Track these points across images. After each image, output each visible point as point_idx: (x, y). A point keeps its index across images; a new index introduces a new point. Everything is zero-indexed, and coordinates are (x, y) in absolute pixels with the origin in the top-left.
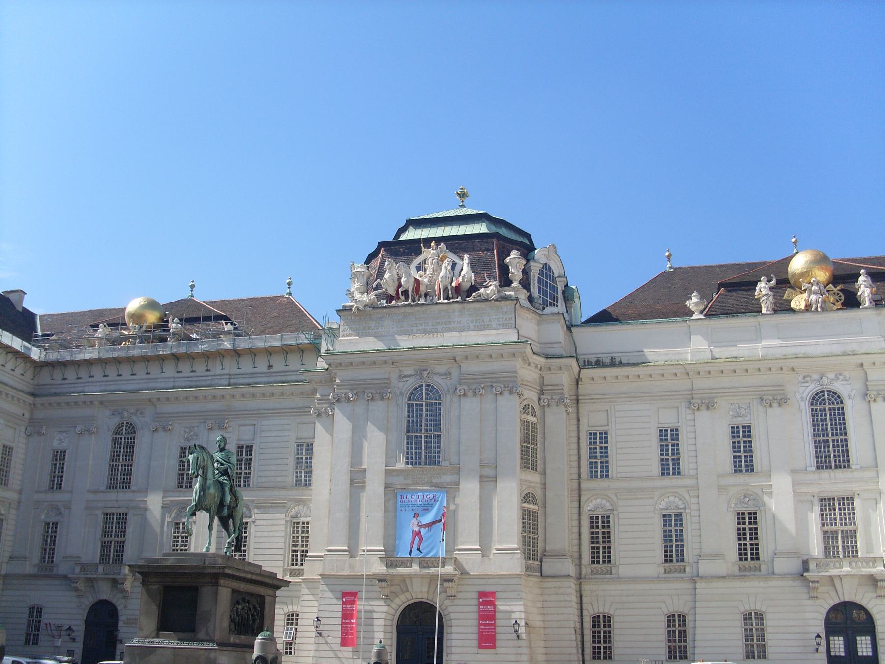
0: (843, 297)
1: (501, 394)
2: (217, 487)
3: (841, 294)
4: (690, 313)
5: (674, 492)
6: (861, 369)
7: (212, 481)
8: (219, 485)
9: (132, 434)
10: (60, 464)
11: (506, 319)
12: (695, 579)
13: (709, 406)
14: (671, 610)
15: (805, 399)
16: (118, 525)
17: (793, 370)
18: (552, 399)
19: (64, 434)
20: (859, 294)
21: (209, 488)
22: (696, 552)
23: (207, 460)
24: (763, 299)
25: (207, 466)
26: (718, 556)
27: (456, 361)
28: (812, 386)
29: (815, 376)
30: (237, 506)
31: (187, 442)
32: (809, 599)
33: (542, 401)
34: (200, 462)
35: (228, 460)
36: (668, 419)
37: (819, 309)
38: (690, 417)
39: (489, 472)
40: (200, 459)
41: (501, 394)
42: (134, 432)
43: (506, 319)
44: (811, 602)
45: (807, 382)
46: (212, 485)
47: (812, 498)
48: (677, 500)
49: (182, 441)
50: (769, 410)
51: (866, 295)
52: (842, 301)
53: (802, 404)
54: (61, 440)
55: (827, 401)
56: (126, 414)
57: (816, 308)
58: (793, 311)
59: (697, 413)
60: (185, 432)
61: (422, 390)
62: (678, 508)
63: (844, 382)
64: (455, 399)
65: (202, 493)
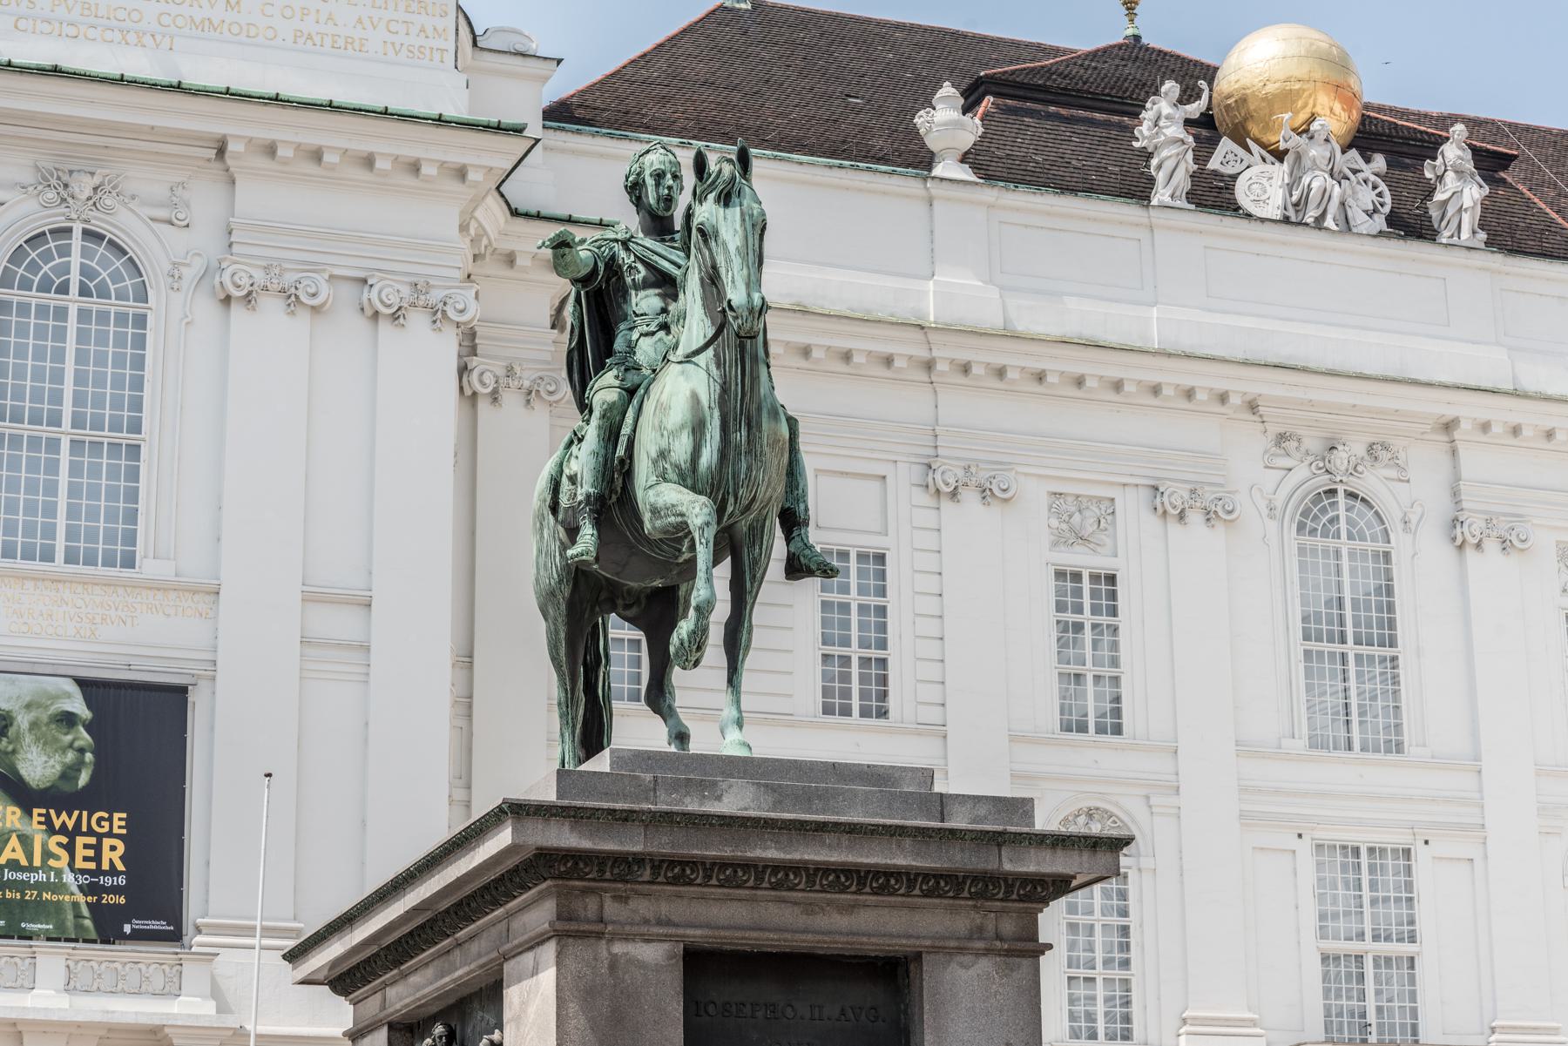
0: (1388, 199)
1: (395, 317)
3: (1383, 187)
4: (920, 160)
6: (1445, 438)
11: (422, 30)
15: (1278, 512)
17: (1253, 407)
18: (510, 371)
20: (1439, 196)
24: (1165, 153)
27: (221, 151)
28: (1301, 472)
29: (1312, 443)
33: (475, 376)
37: (1329, 222)
38: (927, 518)
39: (339, 624)
41: (395, 317)
43: (422, 30)
51: (1467, 203)
52: (1387, 209)
55: (1343, 525)
58: (1249, 216)
59: (946, 505)
61: (65, 251)
63: (1393, 473)
64: (206, 310)
65: (740, 436)
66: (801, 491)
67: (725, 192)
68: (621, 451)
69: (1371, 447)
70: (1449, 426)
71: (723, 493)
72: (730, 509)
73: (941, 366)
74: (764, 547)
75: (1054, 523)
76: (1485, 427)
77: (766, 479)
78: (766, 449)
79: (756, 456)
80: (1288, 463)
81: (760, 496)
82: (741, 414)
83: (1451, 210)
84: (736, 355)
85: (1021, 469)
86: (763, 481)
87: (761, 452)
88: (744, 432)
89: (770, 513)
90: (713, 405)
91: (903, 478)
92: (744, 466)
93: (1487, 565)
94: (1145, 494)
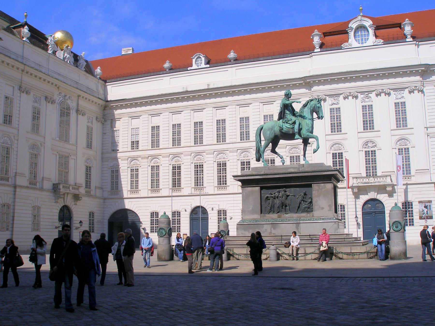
5: (8, 135)
12: (15, 187)
13: (28, 93)
14: (4, 202)
17: (58, 88)
22: (15, 171)
26: (22, 175)
29: (63, 94)
32: (55, 203)
36: (9, 91)
38: (19, 95)
44: (55, 204)
45: (60, 95)
47: (56, 153)
48: (8, 139)
50: (48, 104)
53: (58, 105)
57: (67, 61)
59: (22, 93)
62: (8, 144)
68: (301, 127)
69: (69, 97)
70: (79, 96)
73: (25, 71)
75: (33, 99)
76: (83, 97)
80: (60, 97)
83: (81, 64)
85: (32, 90)
91: (16, 88)
93: (80, 117)
94: (44, 97)
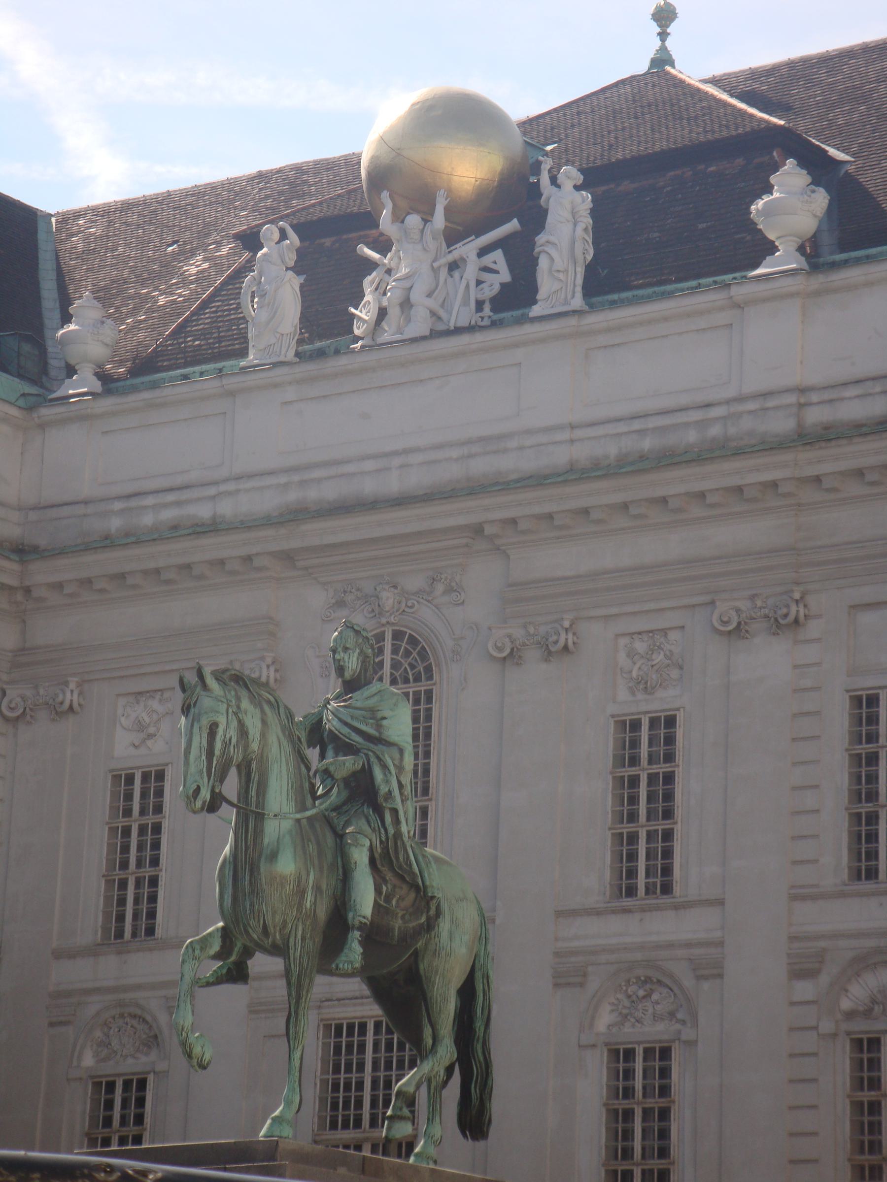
2: (312, 848)
7: (287, 825)
8: (330, 840)
9: (417, 679)
10: (142, 830)
16: (382, 1074)
19: (154, 704)
21: (273, 856)
23: (263, 735)
25: (262, 759)
30: (430, 926)
31: (640, 696)
34: (226, 744)
35: (379, 727)
40: (227, 731)
42: (429, 669)
46: (287, 839)
49: (623, 694)
54: (140, 726)
56: (388, 598)
60: (631, 654)
66: (352, 902)
67: (186, 706)
71: (243, 926)
72: (255, 936)
74: (292, 959)
77: (270, 909)
78: (264, 887)
79: (258, 893)
81: (269, 922)
82: (246, 864)
84: (243, 818)
86: (267, 911)
87: (262, 890)
88: (247, 878)
89: (293, 932)
90: (231, 860)
92: (248, 904)
